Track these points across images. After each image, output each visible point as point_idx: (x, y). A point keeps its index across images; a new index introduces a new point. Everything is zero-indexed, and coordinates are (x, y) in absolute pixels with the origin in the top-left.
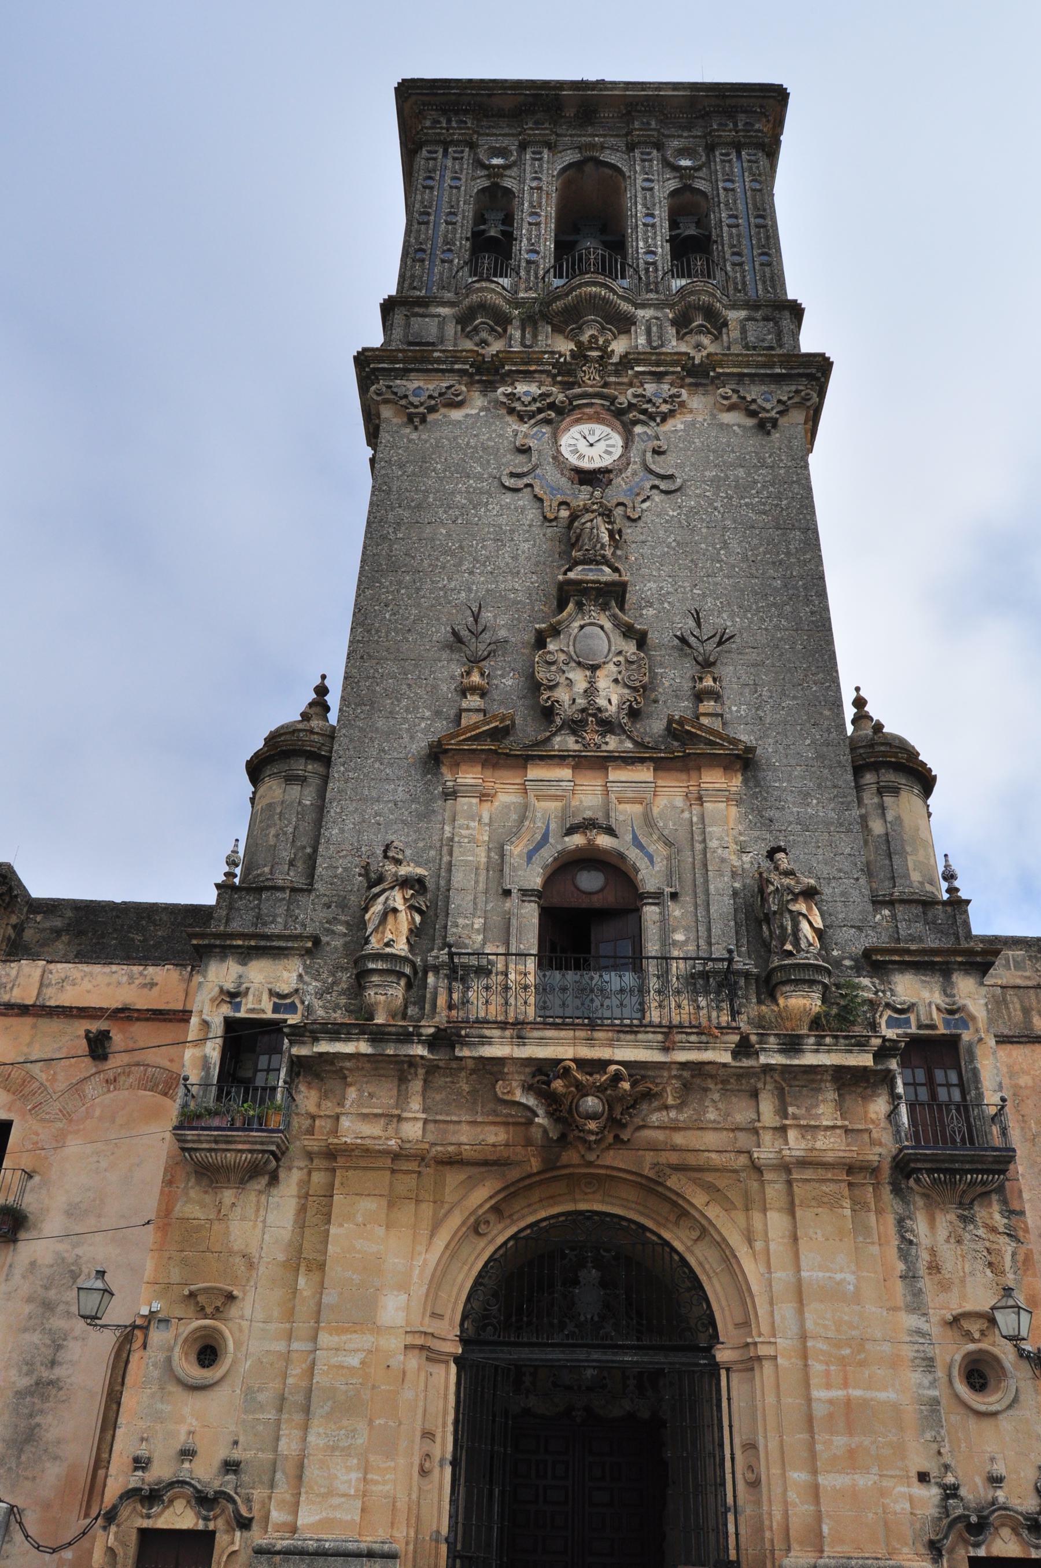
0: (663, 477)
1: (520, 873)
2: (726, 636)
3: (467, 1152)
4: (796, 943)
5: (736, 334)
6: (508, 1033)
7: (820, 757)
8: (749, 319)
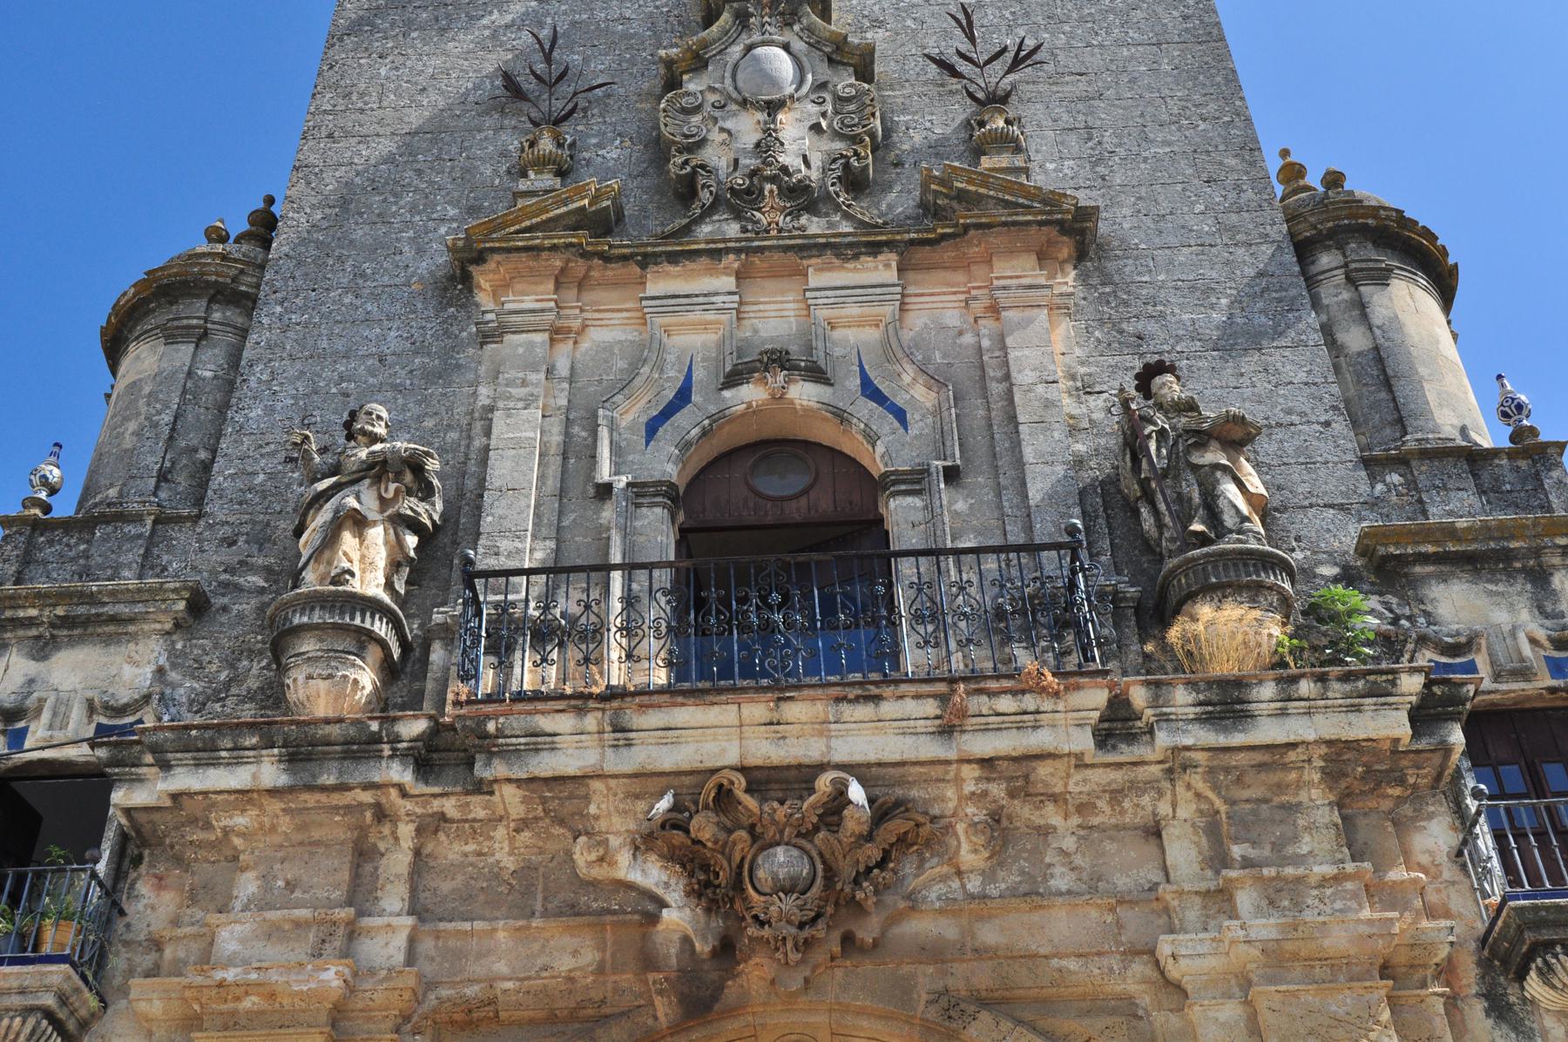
1: (630, 458)
4: (1213, 515)
6: (591, 721)
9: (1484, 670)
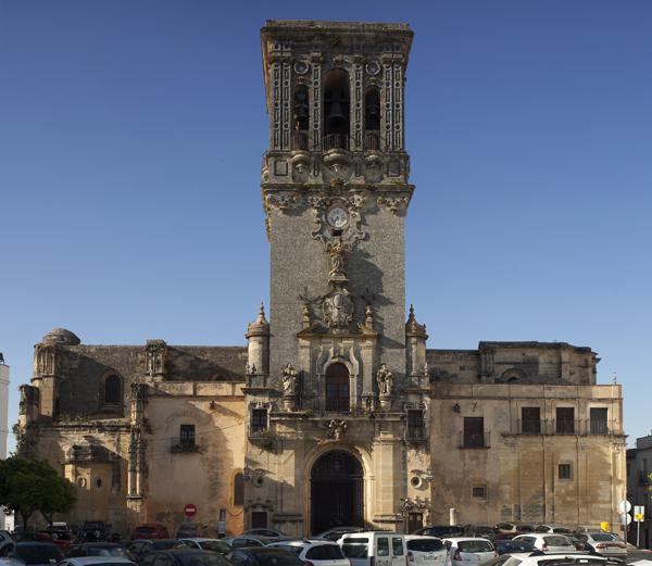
8: (391, 161)
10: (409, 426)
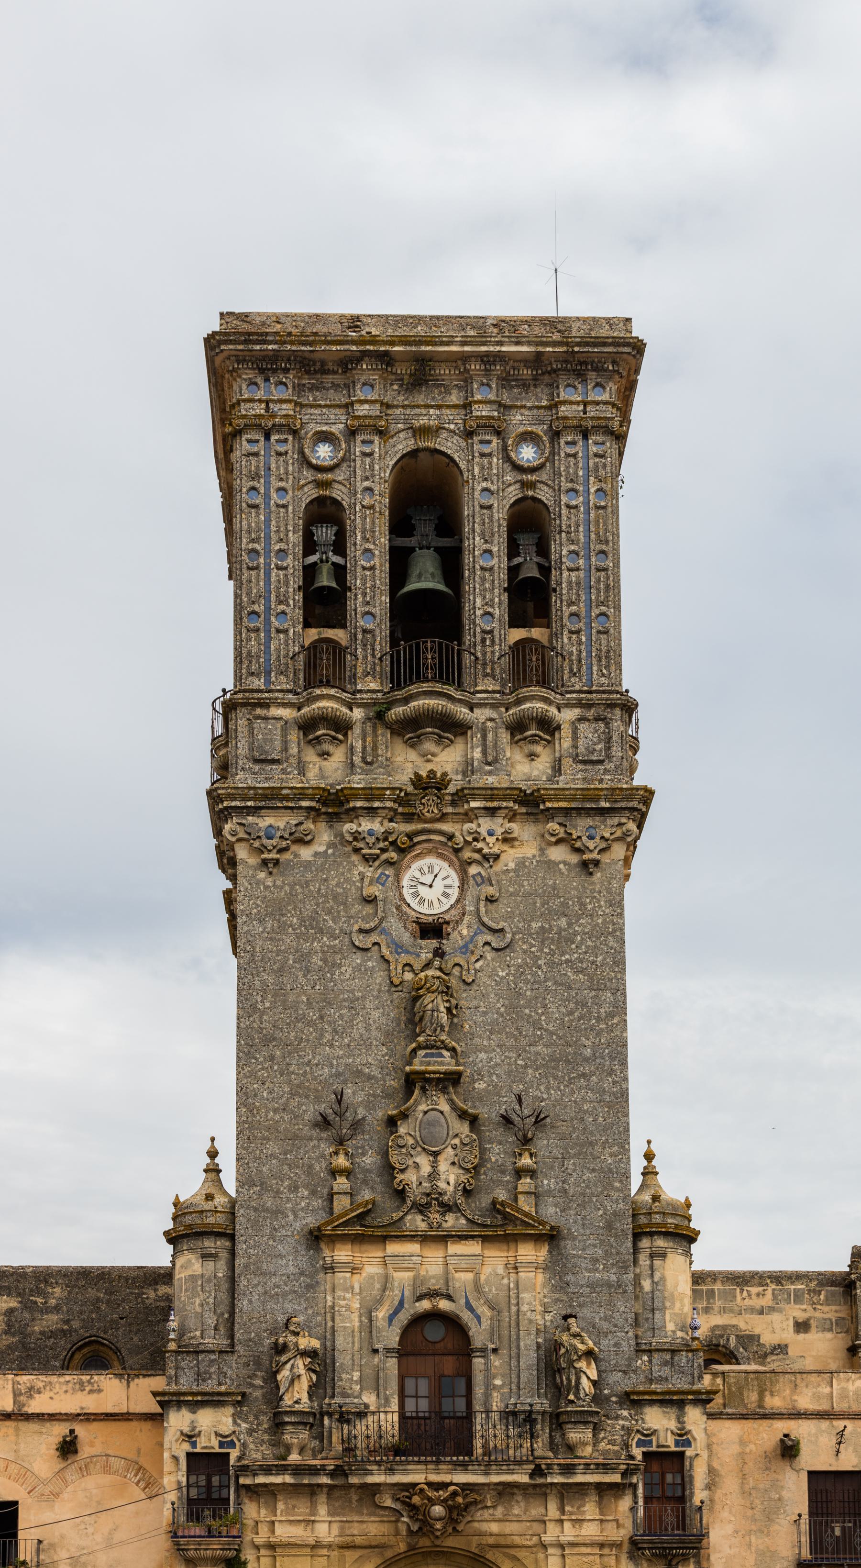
0: (494, 931)
2: (542, 1116)
3: (358, 1540)
4: (577, 1395)
5: (567, 744)
7: (609, 1226)
8: (582, 719)
9: (654, 1444)
10: (647, 1499)
